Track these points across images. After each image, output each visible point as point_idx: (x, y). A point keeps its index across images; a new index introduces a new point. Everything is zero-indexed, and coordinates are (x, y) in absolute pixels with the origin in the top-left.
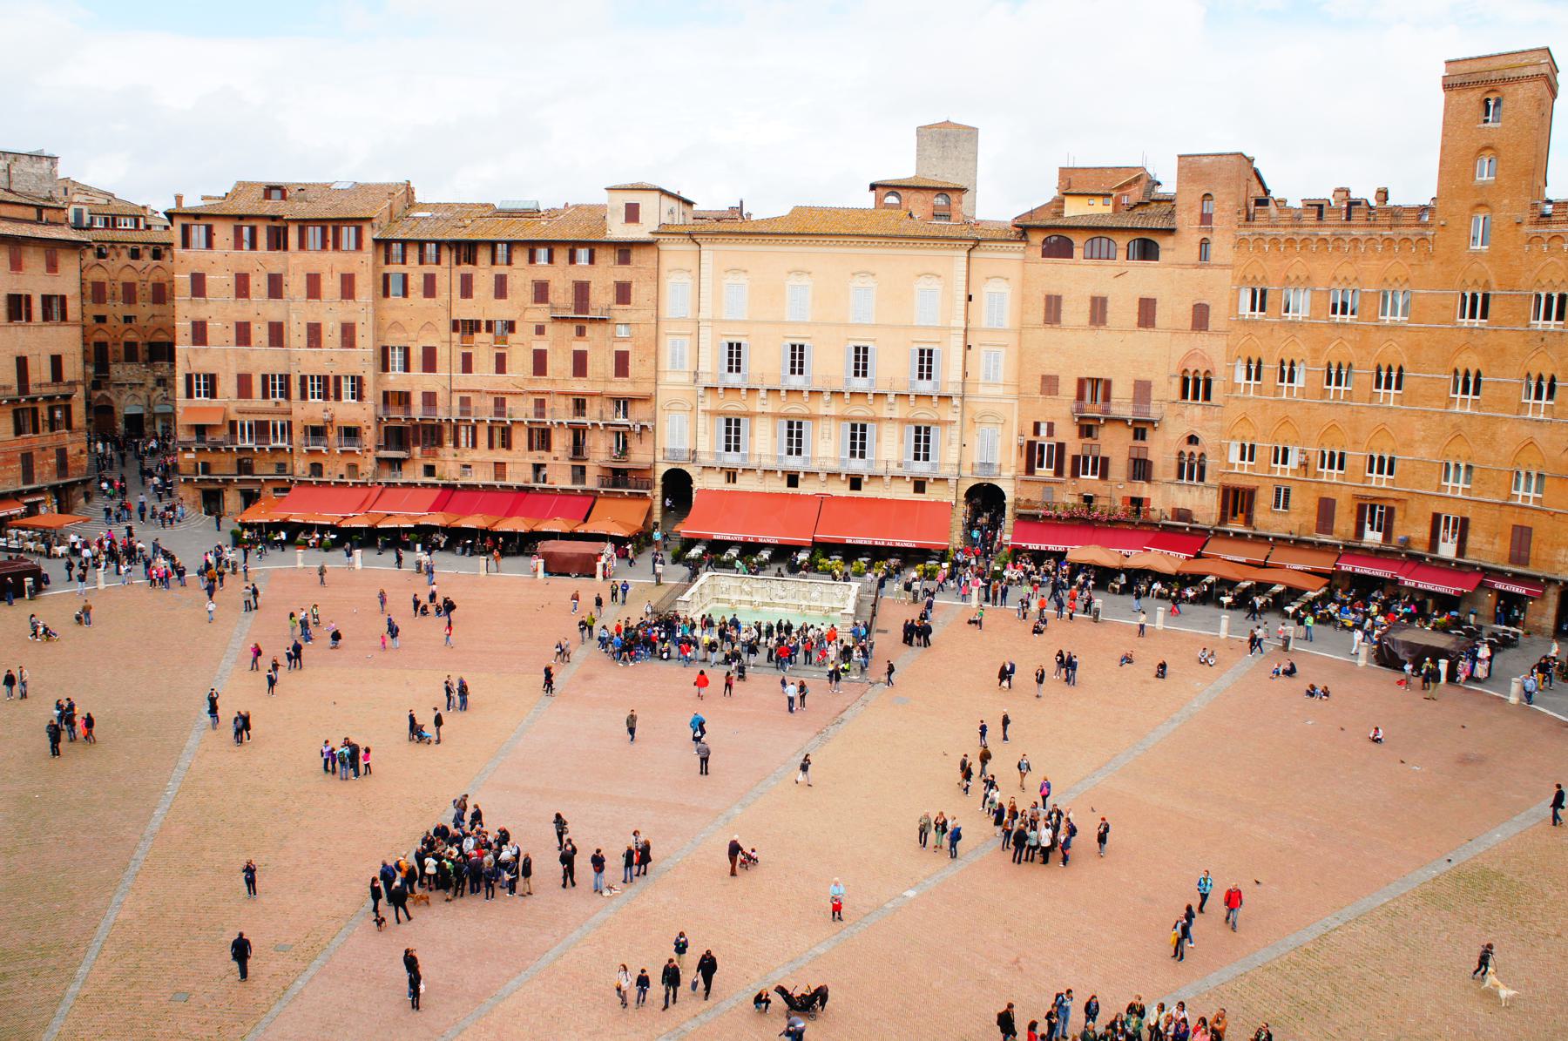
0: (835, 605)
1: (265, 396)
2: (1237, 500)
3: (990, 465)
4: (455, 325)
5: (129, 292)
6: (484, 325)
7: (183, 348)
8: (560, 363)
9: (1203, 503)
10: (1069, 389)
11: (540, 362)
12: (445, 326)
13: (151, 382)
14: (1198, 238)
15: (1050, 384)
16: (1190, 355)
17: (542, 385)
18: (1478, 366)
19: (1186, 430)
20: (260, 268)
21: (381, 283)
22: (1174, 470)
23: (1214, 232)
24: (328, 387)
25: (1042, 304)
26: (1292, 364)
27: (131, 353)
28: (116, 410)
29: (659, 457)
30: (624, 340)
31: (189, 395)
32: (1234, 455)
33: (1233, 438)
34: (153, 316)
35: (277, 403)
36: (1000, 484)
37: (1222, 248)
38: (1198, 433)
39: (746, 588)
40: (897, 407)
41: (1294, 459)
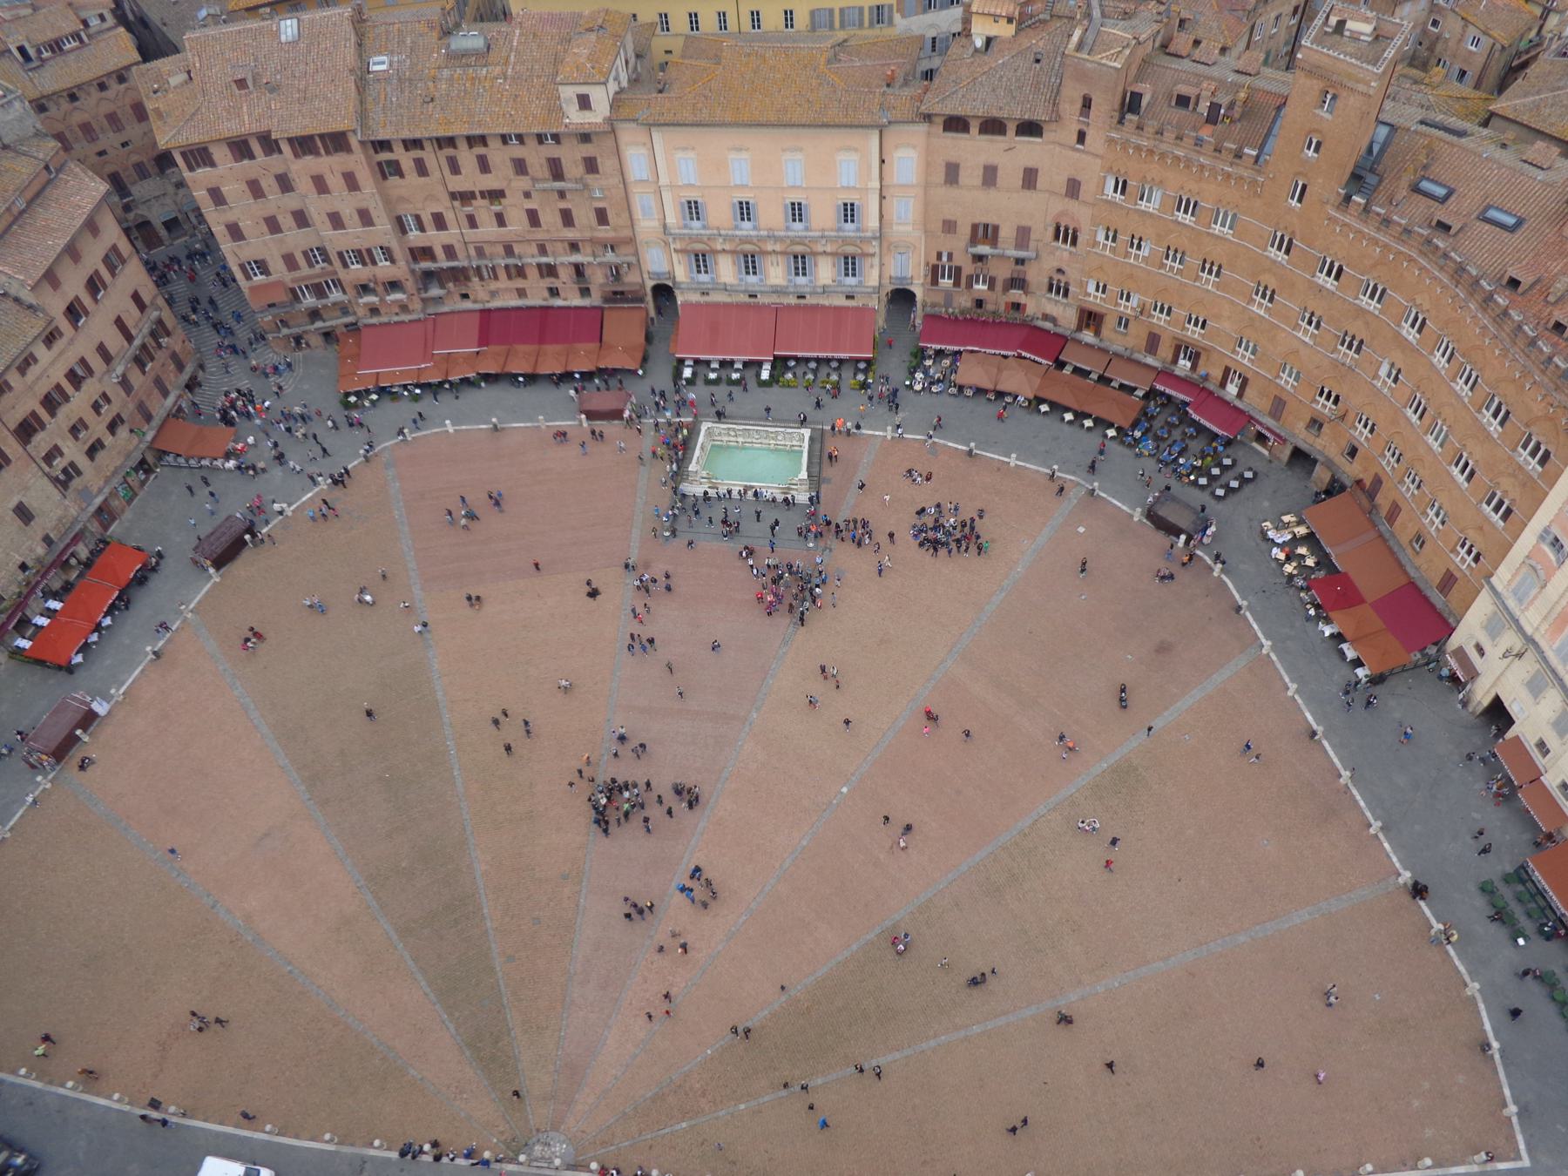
0: (795, 443)
1: (311, 265)
2: (1090, 318)
3: (905, 278)
4: (453, 196)
5: (112, 118)
6: (478, 194)
7: (227, 246)
8: (550, 218)
9: (1065, 315)
10: (965, 231)
11: (533, 218)
12: (446, 198)
13: (171, 189)
14: (1075, 128)
15: (949, 226)
16: (1063, 213)
17: (540, 235)
18: (1274, 287)
19: (1056, 264)
20: (265, 172)
21: (377, 168)
22: (1045, 287)
23: (1090, 127)
24: (365, 257)
25: (944, 169)
26: (1141, 239)
27: (141, 172)
28: (153, 222)
29: (646, 276)
30: (600, 199)
31: (248, 278)
32: (1091, 288)
33: (1092, 277)
34: (145, 133)
35: (322, 268)
36: (912, 289)
37: (1095, 139)
38: (1065, 268)
39: (733, 433)
40: (829, 245)
41: (1134, 302)
